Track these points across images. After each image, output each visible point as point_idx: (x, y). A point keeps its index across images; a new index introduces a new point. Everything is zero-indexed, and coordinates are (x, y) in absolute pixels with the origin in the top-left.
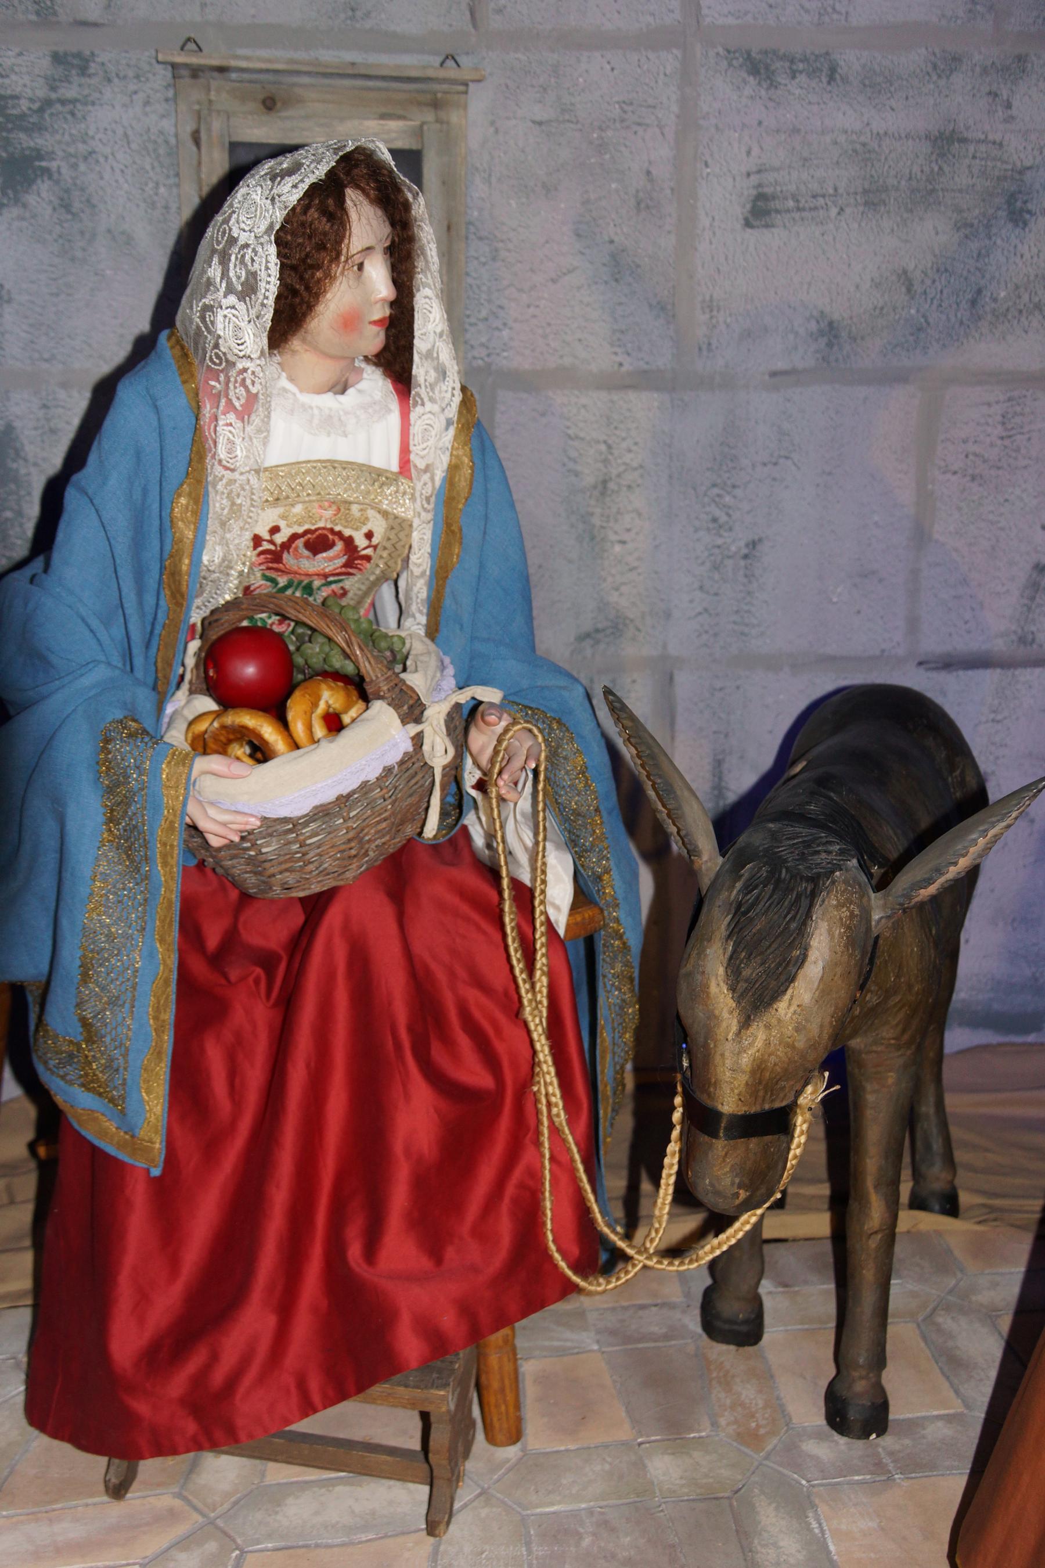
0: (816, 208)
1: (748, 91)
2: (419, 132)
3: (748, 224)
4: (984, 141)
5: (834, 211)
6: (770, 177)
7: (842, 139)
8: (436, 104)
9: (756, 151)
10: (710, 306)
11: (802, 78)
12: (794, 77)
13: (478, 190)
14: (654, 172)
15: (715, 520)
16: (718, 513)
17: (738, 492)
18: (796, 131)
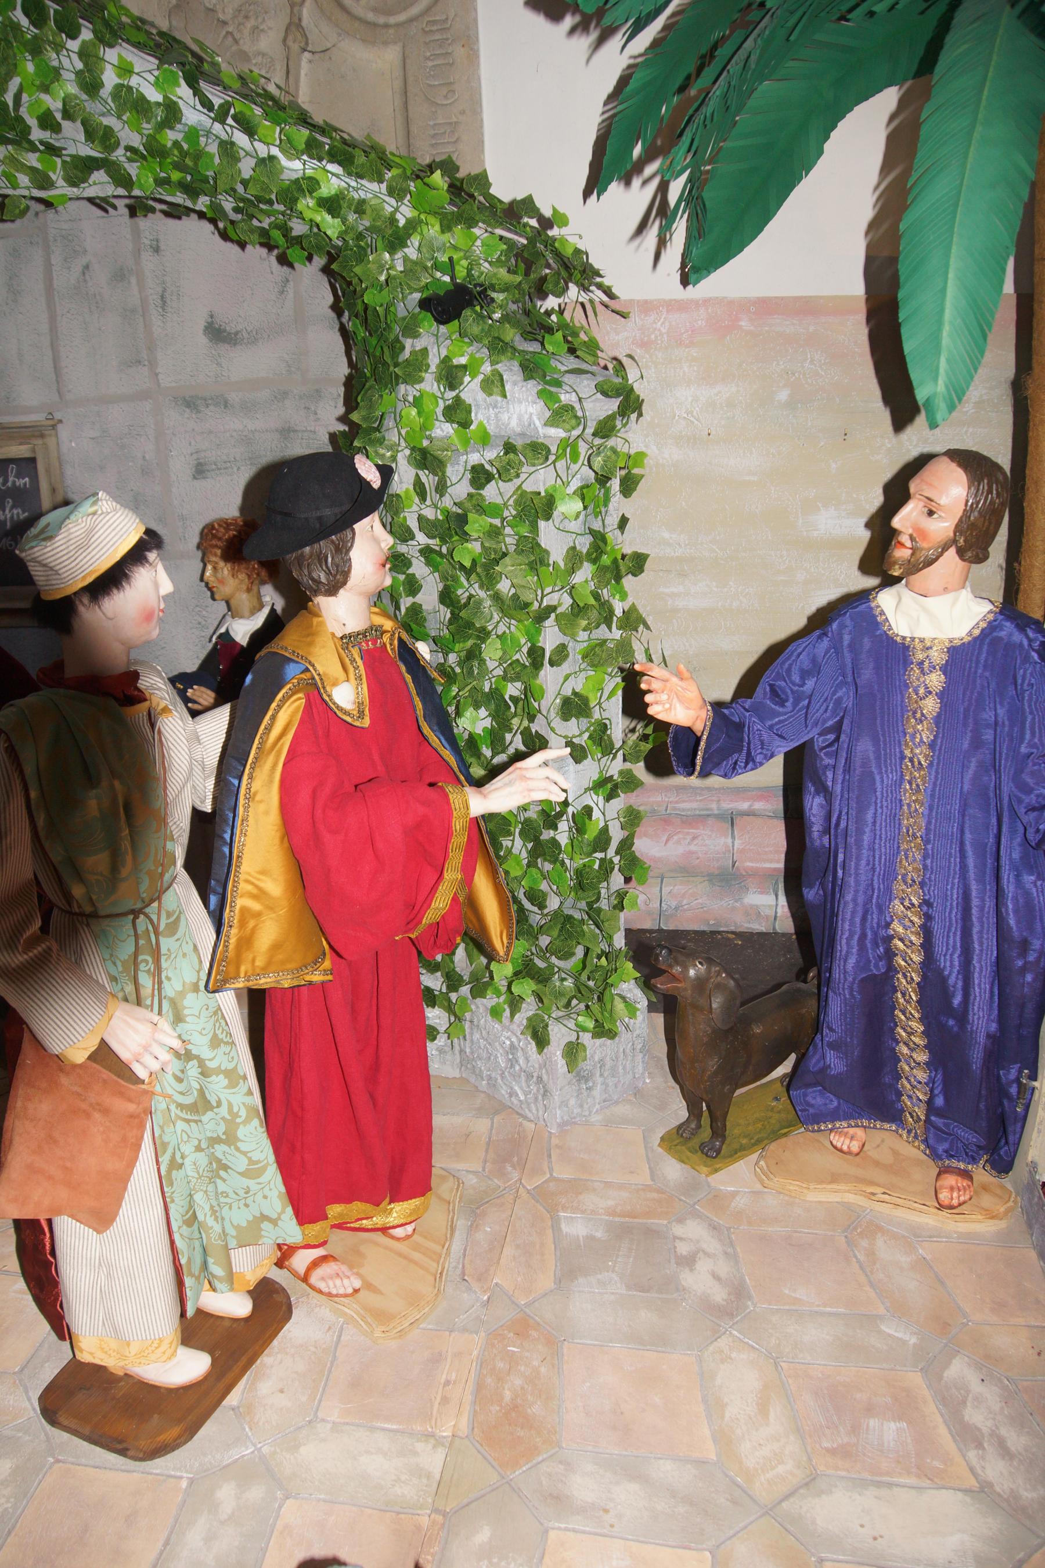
0: (225, 468)
1: (186, 415)
2: (34, 451)
3: (195, 478)
4: (306, 431)
5: (235, 469)
6: (202, 455)
7: (234, 434)
8: (42, 436)
9: (193, 443)
10: (183, 518)
11: (212, 408)
12: (207, 406)
13: (69, 471)
14: (147, 457)
15: (199, 623)
16: (200, 620)
17: (209, 609)
18: (211, 432)
